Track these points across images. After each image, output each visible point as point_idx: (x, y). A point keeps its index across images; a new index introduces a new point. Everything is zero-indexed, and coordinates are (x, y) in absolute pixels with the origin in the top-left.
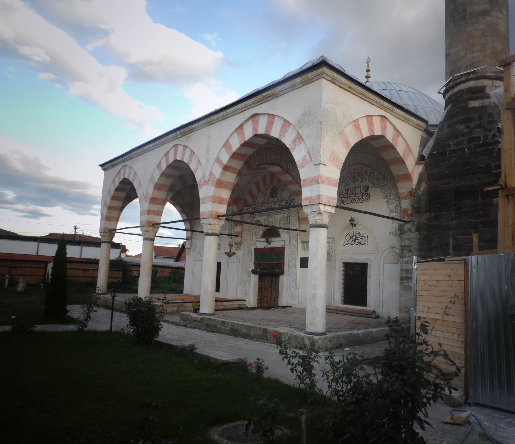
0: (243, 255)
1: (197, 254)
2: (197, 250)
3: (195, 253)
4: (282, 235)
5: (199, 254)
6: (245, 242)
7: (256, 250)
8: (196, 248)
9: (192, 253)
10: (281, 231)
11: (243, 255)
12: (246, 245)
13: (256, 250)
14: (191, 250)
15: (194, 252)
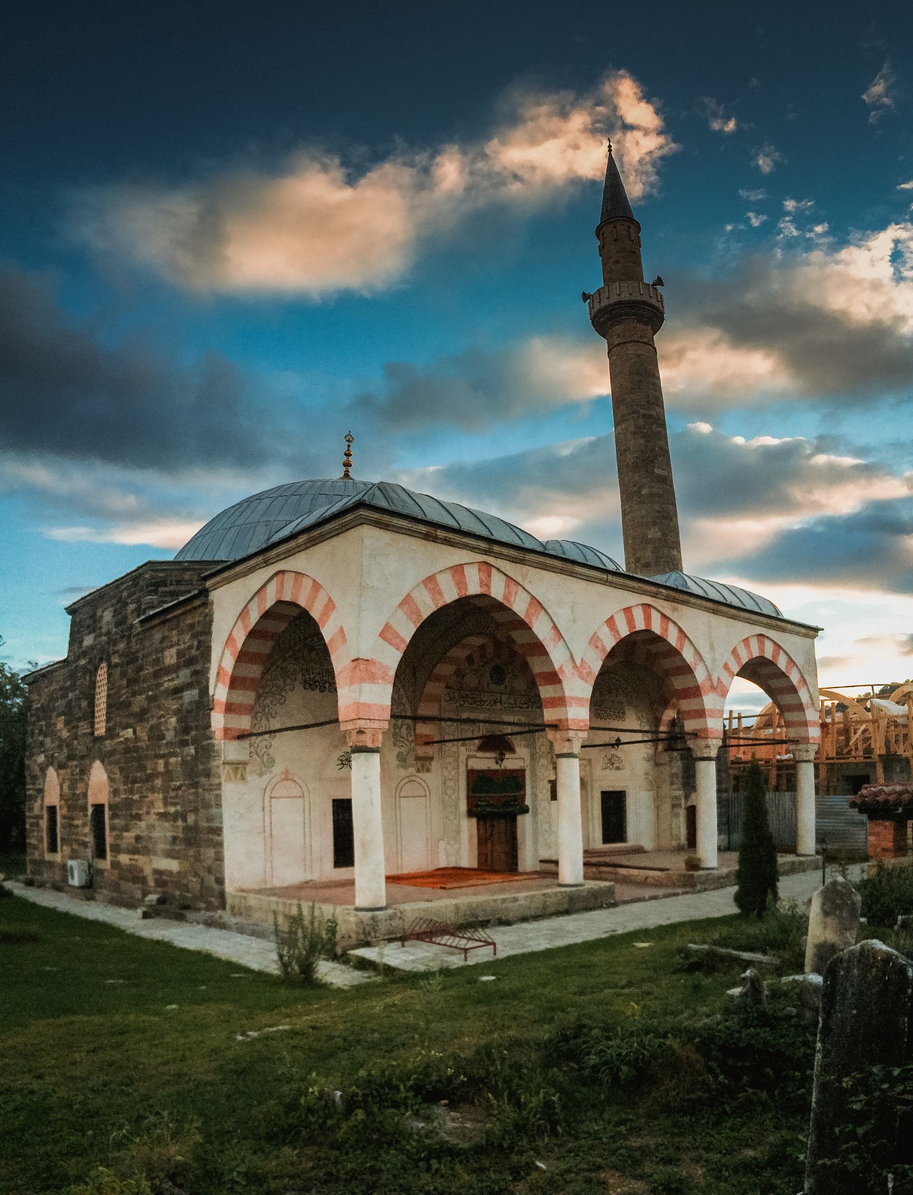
0: (445, 783)
1: (275, 781)
2: (278, 768)
3: (267, 777)
4: (517, 750)
5: (287, 779)
6: (448, 756)
7: (471, 773)
8: (272, 762)
9: (249, 778)
10: (516, 741)
11: (445, 783)
12: (450, 763)
13: (471, 773)
14: (249, 768)
15: (261, 775)
